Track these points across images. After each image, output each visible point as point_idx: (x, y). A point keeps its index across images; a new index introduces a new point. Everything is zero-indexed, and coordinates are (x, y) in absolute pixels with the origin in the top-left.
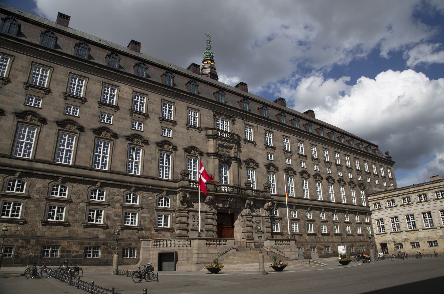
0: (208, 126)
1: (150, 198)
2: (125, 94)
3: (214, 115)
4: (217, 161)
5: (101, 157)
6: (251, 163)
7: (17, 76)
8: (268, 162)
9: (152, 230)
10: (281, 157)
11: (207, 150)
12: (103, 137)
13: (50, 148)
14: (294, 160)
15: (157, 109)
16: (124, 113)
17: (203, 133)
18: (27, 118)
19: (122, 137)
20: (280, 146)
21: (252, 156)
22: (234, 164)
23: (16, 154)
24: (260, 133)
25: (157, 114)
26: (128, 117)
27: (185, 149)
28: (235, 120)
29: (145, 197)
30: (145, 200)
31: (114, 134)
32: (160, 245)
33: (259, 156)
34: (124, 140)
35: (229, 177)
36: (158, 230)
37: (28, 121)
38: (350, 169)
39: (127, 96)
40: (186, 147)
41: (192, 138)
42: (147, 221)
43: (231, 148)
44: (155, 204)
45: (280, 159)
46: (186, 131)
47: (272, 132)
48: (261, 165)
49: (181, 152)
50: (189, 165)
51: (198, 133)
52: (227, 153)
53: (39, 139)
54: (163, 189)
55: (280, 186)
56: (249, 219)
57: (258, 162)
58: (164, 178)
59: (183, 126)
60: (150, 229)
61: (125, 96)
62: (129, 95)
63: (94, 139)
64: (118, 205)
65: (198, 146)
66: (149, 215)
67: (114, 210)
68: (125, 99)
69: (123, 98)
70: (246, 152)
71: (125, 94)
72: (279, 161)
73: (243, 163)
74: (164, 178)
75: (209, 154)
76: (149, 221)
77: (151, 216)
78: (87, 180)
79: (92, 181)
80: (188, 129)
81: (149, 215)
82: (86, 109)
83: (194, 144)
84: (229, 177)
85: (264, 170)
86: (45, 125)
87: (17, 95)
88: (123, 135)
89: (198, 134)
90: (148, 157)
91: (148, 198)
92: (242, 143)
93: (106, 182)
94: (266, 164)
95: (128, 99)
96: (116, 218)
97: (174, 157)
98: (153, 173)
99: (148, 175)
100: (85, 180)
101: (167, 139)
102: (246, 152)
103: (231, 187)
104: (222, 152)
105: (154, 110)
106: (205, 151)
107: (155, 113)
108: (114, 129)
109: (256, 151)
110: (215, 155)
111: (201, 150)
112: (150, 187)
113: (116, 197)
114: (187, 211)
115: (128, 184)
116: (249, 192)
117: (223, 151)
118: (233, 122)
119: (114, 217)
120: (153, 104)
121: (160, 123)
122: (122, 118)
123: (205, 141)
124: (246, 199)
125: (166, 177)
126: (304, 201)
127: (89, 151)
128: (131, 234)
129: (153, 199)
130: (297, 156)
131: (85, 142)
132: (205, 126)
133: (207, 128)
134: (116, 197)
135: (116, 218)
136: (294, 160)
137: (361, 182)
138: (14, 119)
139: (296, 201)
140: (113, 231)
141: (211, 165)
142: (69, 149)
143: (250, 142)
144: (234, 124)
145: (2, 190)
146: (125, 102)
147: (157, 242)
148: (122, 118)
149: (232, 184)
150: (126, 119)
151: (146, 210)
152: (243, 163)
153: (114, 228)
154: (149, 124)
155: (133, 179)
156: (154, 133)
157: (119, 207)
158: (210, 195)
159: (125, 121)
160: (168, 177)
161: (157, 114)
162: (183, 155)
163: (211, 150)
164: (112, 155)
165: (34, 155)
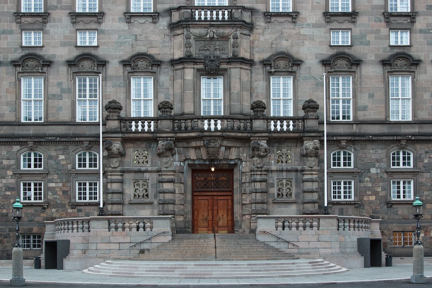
1: (62, 157)
9: (67, 207)
10: (378, 32)
14: (421, 31)
17: (164, 22)
21: (285, 45)
26: (14, 26)
29: (52, 156)
30: (52, 162)
32: (78, 228)
33: (306, 43)
36: (74, 206)
40: (125, 58)
41: (138, 37)
42: (58, 193)
45: (370, 38)
54: (81, 139)
56: (258, 178)
59: (120, 19)
60: (63, 206)
64: (10, 173)
65: (152, 52)
66: (61, 185)
67: (4, 181)
72: (368, 43)
76: (61, 193)
77: (63, 186)
80: (129, 23)
81: (61, 185)
83: (142, 49)
85: (320, 72)
88: (9, 60)
89: (151, 27)
91: (58, 157)
94: (324, 57)
96: (8, 193)
97: (105, 79)
98: (65, 116)
99: (56, 120)
107: (61, 9)
109: (299, 34)
119: (6, 190)
121: (73, 23)
123: (167, 39)
128: (33, 214)
129: (66, 159)
134: (5, 162)
135: (8, 193)
136: (421, 31)
140: (5, 211)
147: (73, 224)
149: (227, 114)
150: (11, 32)
151: (56, 177)
153: (6, 207)
154: (52, 30)
155: (31, 131)
156: (63, 44)
159: (9, 36)
162: (121, 74)
163: (179, 54)
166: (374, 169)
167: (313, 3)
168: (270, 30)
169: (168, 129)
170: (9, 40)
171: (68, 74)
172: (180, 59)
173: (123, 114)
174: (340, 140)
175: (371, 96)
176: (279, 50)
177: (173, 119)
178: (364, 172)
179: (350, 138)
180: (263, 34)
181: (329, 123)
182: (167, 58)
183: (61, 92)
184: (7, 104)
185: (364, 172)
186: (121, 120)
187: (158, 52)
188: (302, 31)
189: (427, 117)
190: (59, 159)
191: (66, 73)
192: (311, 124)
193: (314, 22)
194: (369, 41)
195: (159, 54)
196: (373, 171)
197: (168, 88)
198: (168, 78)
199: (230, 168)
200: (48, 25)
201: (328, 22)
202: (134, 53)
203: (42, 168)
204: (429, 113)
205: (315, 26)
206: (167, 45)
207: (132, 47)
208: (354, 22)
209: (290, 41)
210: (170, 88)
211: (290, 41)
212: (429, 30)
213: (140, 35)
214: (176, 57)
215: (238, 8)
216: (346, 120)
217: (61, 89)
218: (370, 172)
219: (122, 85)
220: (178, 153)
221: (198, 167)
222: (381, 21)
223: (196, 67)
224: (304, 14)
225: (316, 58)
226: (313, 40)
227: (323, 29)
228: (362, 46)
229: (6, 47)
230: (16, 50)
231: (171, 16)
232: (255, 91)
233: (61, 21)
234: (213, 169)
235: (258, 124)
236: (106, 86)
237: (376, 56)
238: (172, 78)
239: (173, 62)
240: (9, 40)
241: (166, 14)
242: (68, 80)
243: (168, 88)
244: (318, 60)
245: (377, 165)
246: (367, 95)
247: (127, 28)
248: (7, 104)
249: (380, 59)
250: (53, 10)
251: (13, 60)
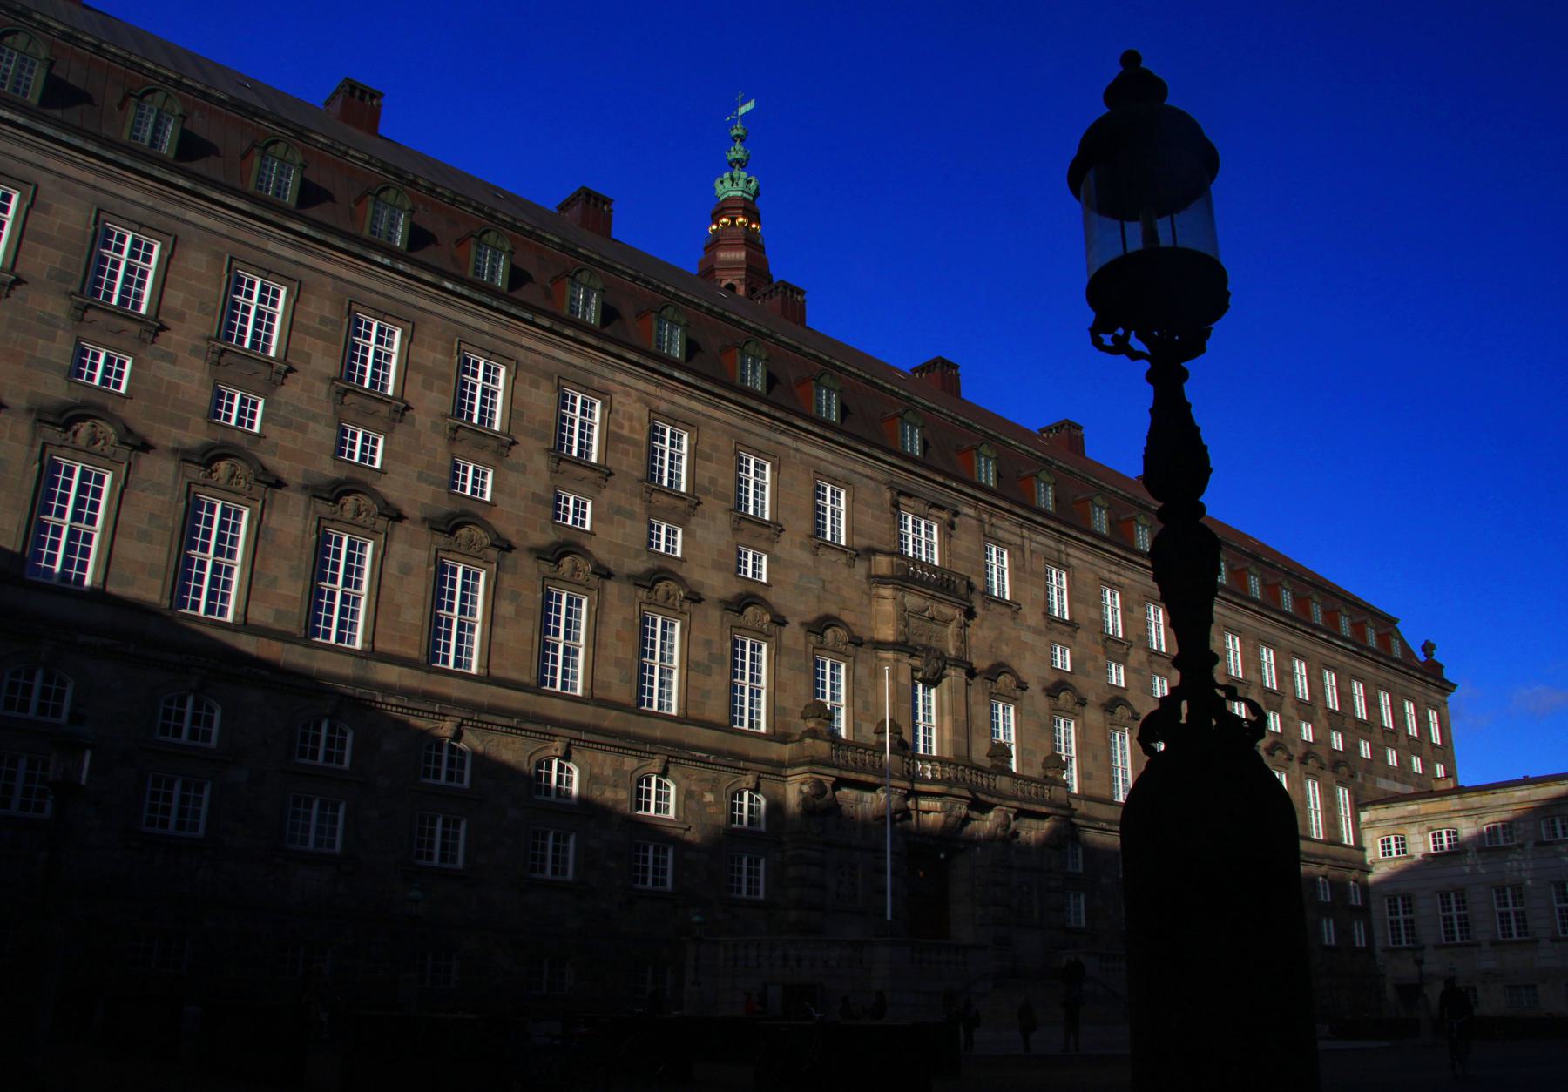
0: (875, 544)
2: (627, 424)
7: (309, 355)
8: (1054, 678)
10: (1095, 659)
11: (872, 630)
12: (567, 575)
13: (414, 615)
14: (1135, 671)
15: (721, 481)
25: (724, 497)
30: (693, 804)
31: (691, 592)
33: (1028, 655)
34: (423, 532)
38: (1307, 710)
39: (632, 430)
40: (809, 617)
48: (1035, 688)
53: (384, 581)
57: (1024, 678)
59: (802, 544)
61: (625, 432)
62: (638, 426)
65: (847, 617)
71: (627, 424)
72: (1088, 676)
75: (881, 645)
82: (513, 478)
83: (833, 610)
85: (1042, 702)
87: (311, 424)
88: (625, 570)
89: (845, 572)
90: (699, 654)
94: (1048, 684)
95: (635, 443)
98: (715, 710)
101: (753, 588)
106: (866, 636)
107: (717, 496)
110: (897, 646)
116: (1003, 783)
120: (709, 459)
122: (619, 511)
127: (529, 628)
130: (1143, 656)
133: (871, 552)
136: (1135, 671)
137: (1341, 757)
138: (308, 508)
143: (1000, 601)
146: (625, 453)
149: (947, 754)
150: (631, 515)
154: (699, 533)
159: (628, 522)
162: (801, 647)
164: (594, 642)
165: (241, 611)
184: (618, 663)
200: (693, 520)
202: (821, 613)
224: (1025, 609)
233: (714, 519)
247: (810, 563)
248: (618, 663)
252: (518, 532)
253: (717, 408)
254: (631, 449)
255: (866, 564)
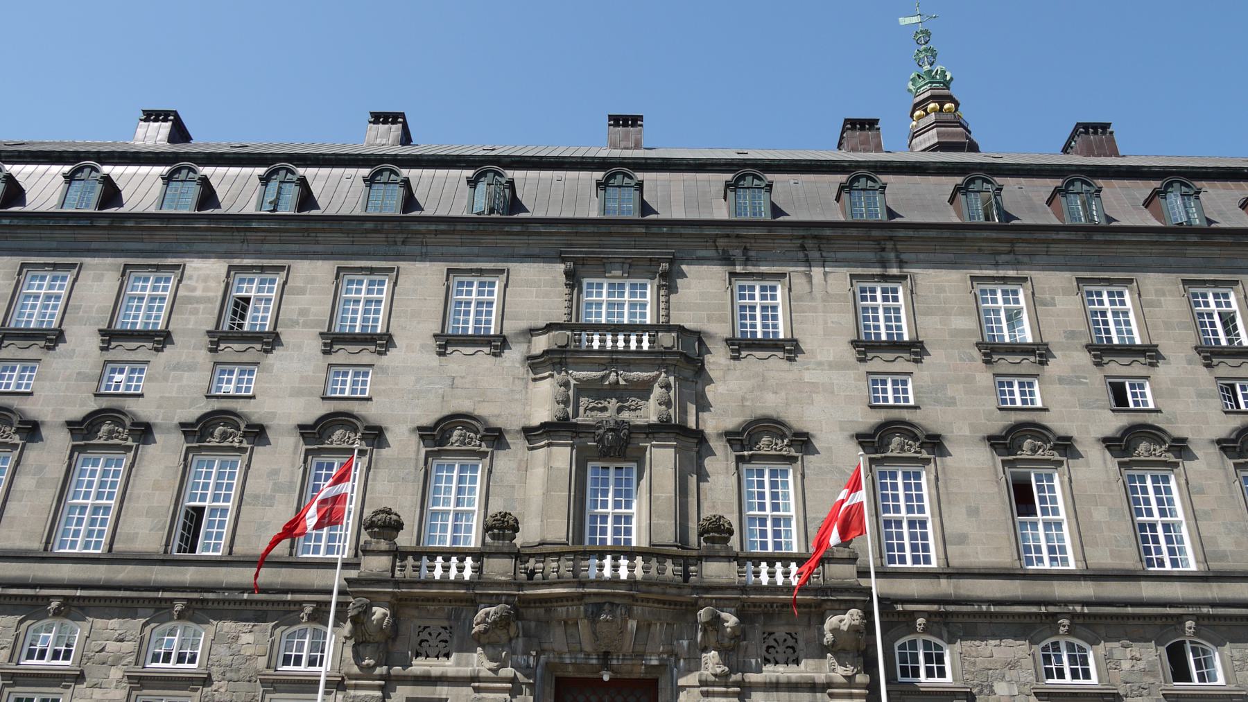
1: (247, 638)
2: (200, 286)
3: (568, 274)
4: (562, 456)
5: (769, 523)
6: (770, 441)
8: (879, 417)
10: (969, 380)
14: (1061, 380)
15: (314, 309)
16: (190, 349)
17: (515, 355)
18: (212, 435)
19: (168, 430)
20: (956, 333)
21: (770, 404)
22: (662, 459)
23: (62, 546)
24: (827, 296)
26: (203, 357)
27: (420, 429)
28: (683, 275)
30: (221, 651)
35: (639, 512)
37: (214, 442)
39: (205, 289)
40: (428, 420)
43: (643, 389)
44: (262, 662)
46: (434, 360)
47: (1022, 280)
49: (403, 445)
50: (1137, 501)
51: (491, 358)
52: (625, 415)
55: (958, 522)
58: (909, 564)
59: (423, 346)
61: (198, 293)
62: (213, 284)
63: (733, 465)
64: (116, 673)
65: (483, 410)
68: (198, 300)
69: (189, 300)
70: (734, 390)
72: (952, 402)
73: (718, 446)
74: (909, 564)
78: (16, 596)
79: (32, 597)
83: (464, 406)
84: (639, 512)
86: (501, 452)
92: (718, 359)
93: (79, 593)
94: (862, 429)
100: (11, 596)
102: (734, 390)
103: (800, 561)
104: (599, 415)
105: (303, 312)
107: (305, 325)
108: (143, 410)
111: (497, 423)
112: (246, 596)
113: (112, 646)
114: (381, 677)
115: (160, 595)
117: (604, 409)
118: (669, 282)
120: (302, 291)
121: (325, 352)
122: (177, 367)
123: (519, 385)
124: (695, 606)
125: (916, 560)
126: (1148, 590)
129: (256, 643)
131: (40, 469)
132: (524, 325)
134: (112, 646)
136: (1061, 380)
139: (1087, 590)
141: (538, 474)
142: (623, 510)
144: (671, 289)
145: (136, 664)
146: (195, 312)
148: (177, 367)
149: (645, 544)
150: (191, 368)
152: (718, 446)
156: (297, 393)
157: (119, 681)
158: (493, 600)
159: (186, 374)
160: (927, 560)
161: (317, 323)
162: (413, 455)
163: (543, 413)
166: (1004, 684)
167: (826, 323)
168: (738, 373)
169: (502, 575)
170: (185, 382)
171: (294, 453)
172: (544, 425)
173: (405, 539)
174: (913, 612)
175: (973, 512)
176: (760, 412)
177: (519, 556)
178: (981, 692)
179: (935, 607)
180: (724, 379)
181: (878, 575)
182: (517, 424)
183: (274, 490)
185: (981, 692)
186: (399, 554)
187: (496, 412)
188: (808, 376)
189: (1110, 561)
190: (240, 642)
191: (291, 449)
192: (840, 573)
193: (831, 359)
194: (954, 398)
195: (499, 416)
196: (1001, 689)
197: (513, 487)
198: (514, 465)
199: (649, 676)
201: (860, 360)
202: (446, 413)
203: (195, 666)
204: (1111, 552)
205: (835, 365)
206: (517, 396)
207: (443, 400)
208: (916, 361)
209: (783, 394)
210: (517, 486)
211: (783, 394)
212: (1077, 377)
213: (462, 377)
214: (536, 421)
215: (668, 328)
216: (922, 565)
217: (275, 484)
218: (992, 692)
219: (412, 477)
220: (524, 636)
221: (571, 672)
222: (972, 359)
223: (577, 441)
225: (842, 429)
226: (833, 392)
227: (851, 373)
228: (938, 408)
229: (174, 394)
230: (193, 402)
231: (530, 342)
232: (709, 496)
233: (299, 347)
234: (606, 678)
235: (716, 571)
236: (374, 480)
237: (973, 427)
238: (523, 464)
239: (530, 433)
240: (185, 382)
241: (521, 339)
242: (293, 466)
243: (513, 487)
244: (847, 434)
245: (1009, 675)
246: (964, 510)
249: (981, 434)
250: (286, 326)
251: (183, 421)
252: (53, 411)
253: (317, 242)
254: (202, 306)
255: (525, 346)
